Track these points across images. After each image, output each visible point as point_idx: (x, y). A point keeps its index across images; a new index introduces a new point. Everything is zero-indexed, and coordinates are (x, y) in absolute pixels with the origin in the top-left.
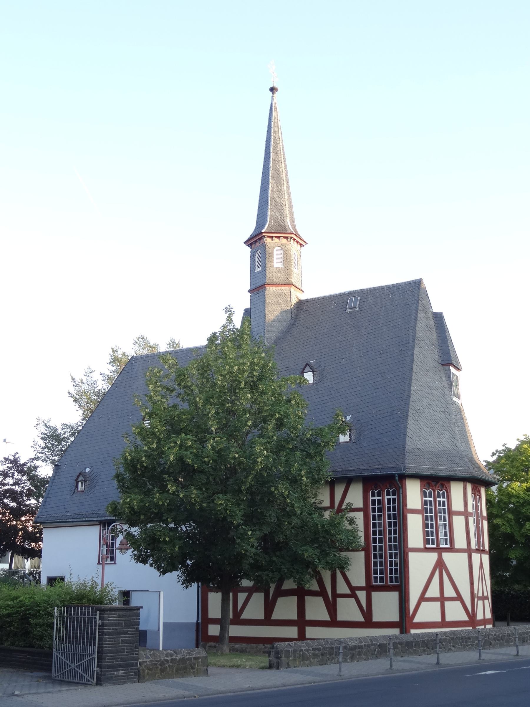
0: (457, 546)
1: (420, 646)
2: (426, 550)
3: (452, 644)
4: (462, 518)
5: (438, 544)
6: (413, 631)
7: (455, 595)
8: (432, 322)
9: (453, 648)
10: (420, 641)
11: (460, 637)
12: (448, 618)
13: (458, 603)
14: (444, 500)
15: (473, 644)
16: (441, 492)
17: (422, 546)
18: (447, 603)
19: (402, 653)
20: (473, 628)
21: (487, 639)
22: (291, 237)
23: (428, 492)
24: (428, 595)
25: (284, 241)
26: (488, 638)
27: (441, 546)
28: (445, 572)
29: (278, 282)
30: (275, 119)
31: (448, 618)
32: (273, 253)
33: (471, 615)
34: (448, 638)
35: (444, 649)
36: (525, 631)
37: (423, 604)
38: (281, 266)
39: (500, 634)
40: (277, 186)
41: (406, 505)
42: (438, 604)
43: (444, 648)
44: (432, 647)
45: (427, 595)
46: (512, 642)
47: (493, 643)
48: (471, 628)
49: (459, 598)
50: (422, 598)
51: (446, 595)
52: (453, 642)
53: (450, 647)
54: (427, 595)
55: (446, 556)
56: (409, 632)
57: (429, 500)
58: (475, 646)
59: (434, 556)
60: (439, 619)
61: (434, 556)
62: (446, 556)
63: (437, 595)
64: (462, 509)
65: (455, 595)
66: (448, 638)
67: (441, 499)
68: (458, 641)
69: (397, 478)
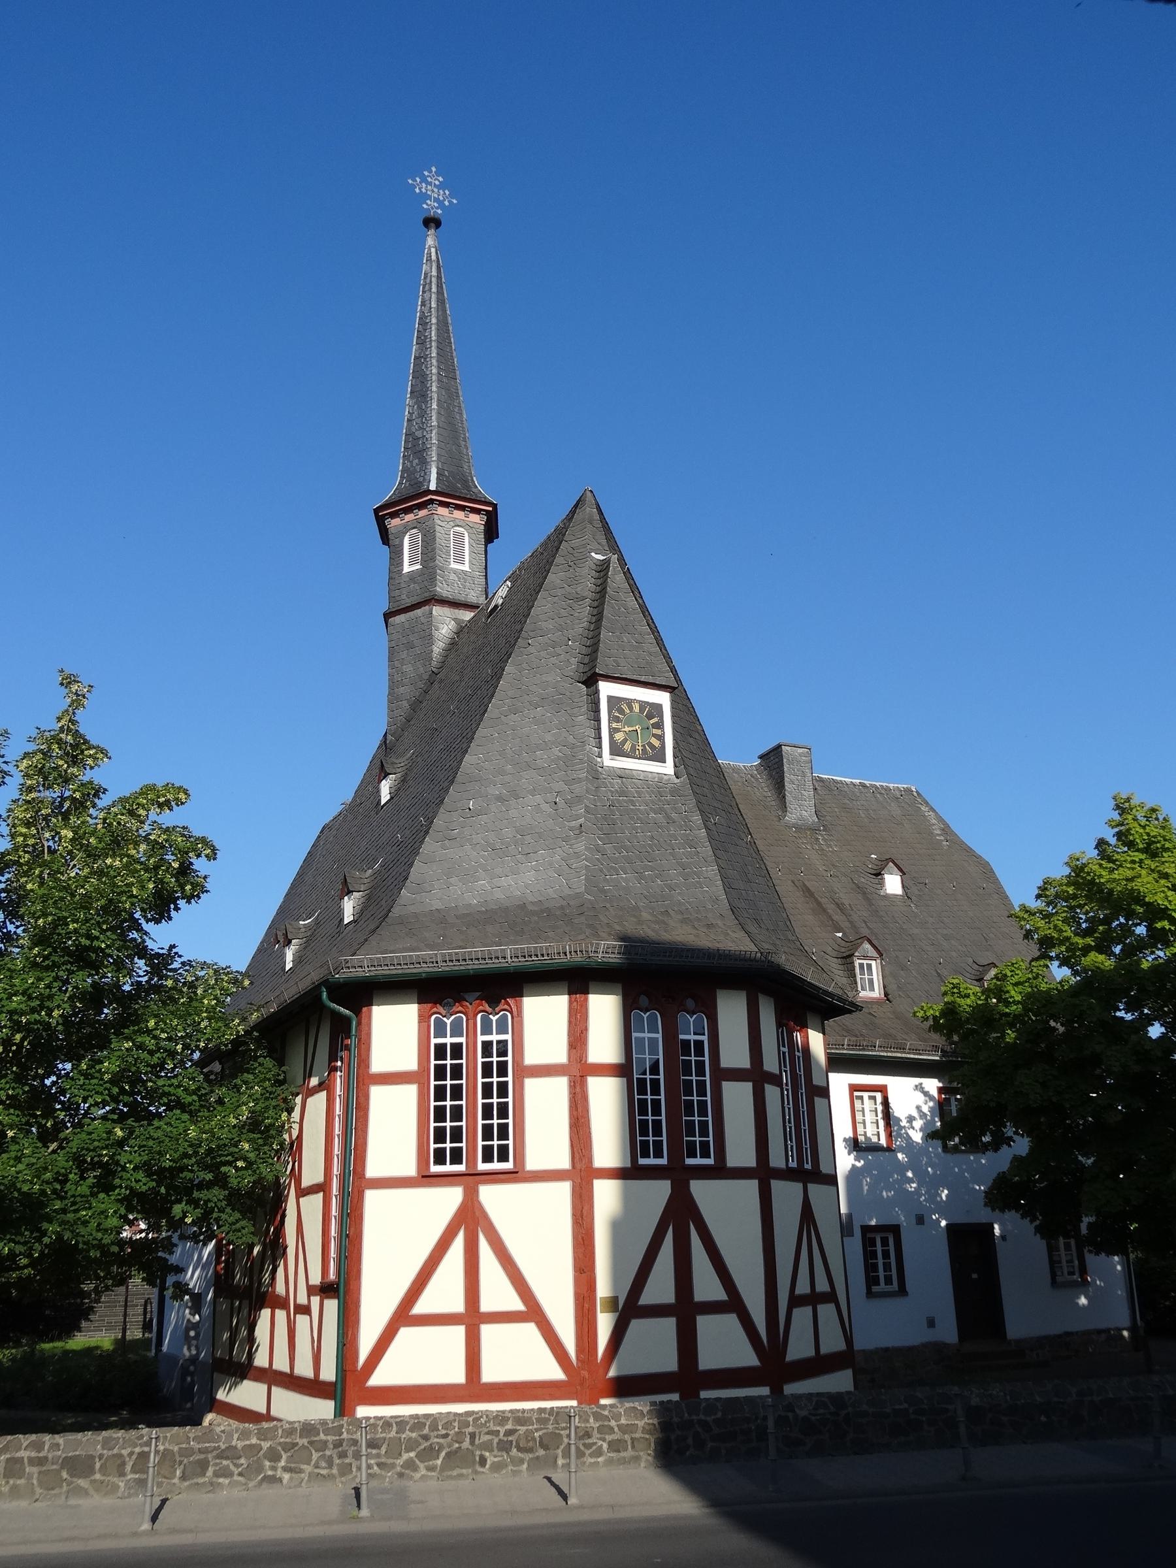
0: (533, 1163)
1: (128, 1468)
2: (425, 1179)
3: (282, 1463)
4: (560, 1086)
5: (472, 1162)
6: (363, 1411)
7: (517, 1305)
8: (588, 585)
9: (286, 1477)
10: (131, 1454)
11: (326, 1442)
12: (490, 1374)
13: (531, 1329)
14: (487, 1038)
15: (390, 1461)
16: (494, 1018)
17: (410, 1169)
18: (487, 1331)
19: (38, 1491)
20: (580, 1403)
21: (466, 1444)
22: (432, 501)
23: (448, 1022)
24: (646, 1299)
25: (423, 513)
26: (472, 1442)
27: (482, 1167)
28: (487, 1240)
29: (409, 602)
30: (425, 278)
31: (490, 1374)
32: (402, 545)
33: (575, 1364)
34: (266, 1445)
35: (240, 1478)
36: (676, 1419)
37: (405, 1334)
38: (418, 567)
39: (537, 1430)
40: (420, 408)
41: (368, 1066)
42: (460, 1331)
43: (240, 1474)
44: (183, 1473)
45: (421, 1307)
46: (599, 1452)
47: (491, 1459)
48: (574, 1403)
49: (533, 1313)
50: (403, 1316)
51: (487, 1304)
52: (288, 1457)
53: (270, 1473)
54: (419, 1308)
55: (491, 1196)
56: (354, 1411)
57: (695, 1041)
58: (399, 1469)
59: (453, 1196)
60: (457, 1375)
61: (453, 1196)
62: (491, 1196)
63: (457, 1305)
64: (559, 1054)
65: (517, 1305)
66: (266, 1445)
67: (494, 1038)
68: (315, 1456)
69: (325, 995)
